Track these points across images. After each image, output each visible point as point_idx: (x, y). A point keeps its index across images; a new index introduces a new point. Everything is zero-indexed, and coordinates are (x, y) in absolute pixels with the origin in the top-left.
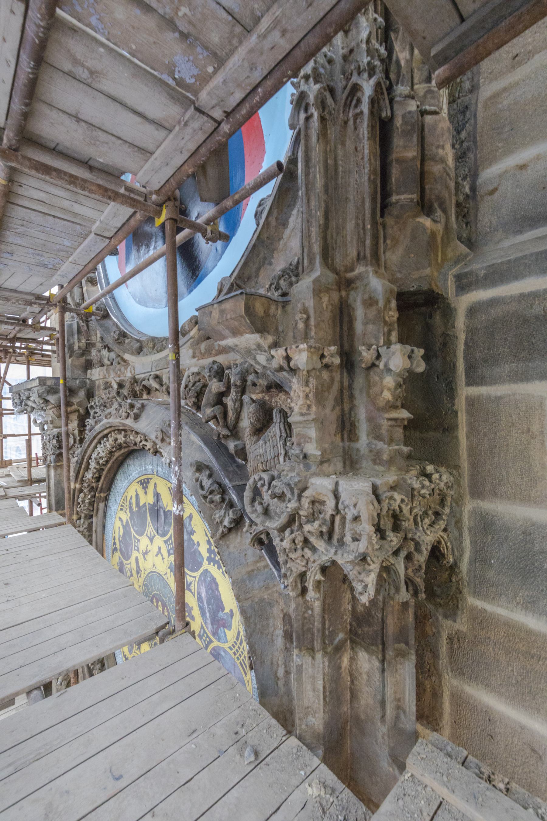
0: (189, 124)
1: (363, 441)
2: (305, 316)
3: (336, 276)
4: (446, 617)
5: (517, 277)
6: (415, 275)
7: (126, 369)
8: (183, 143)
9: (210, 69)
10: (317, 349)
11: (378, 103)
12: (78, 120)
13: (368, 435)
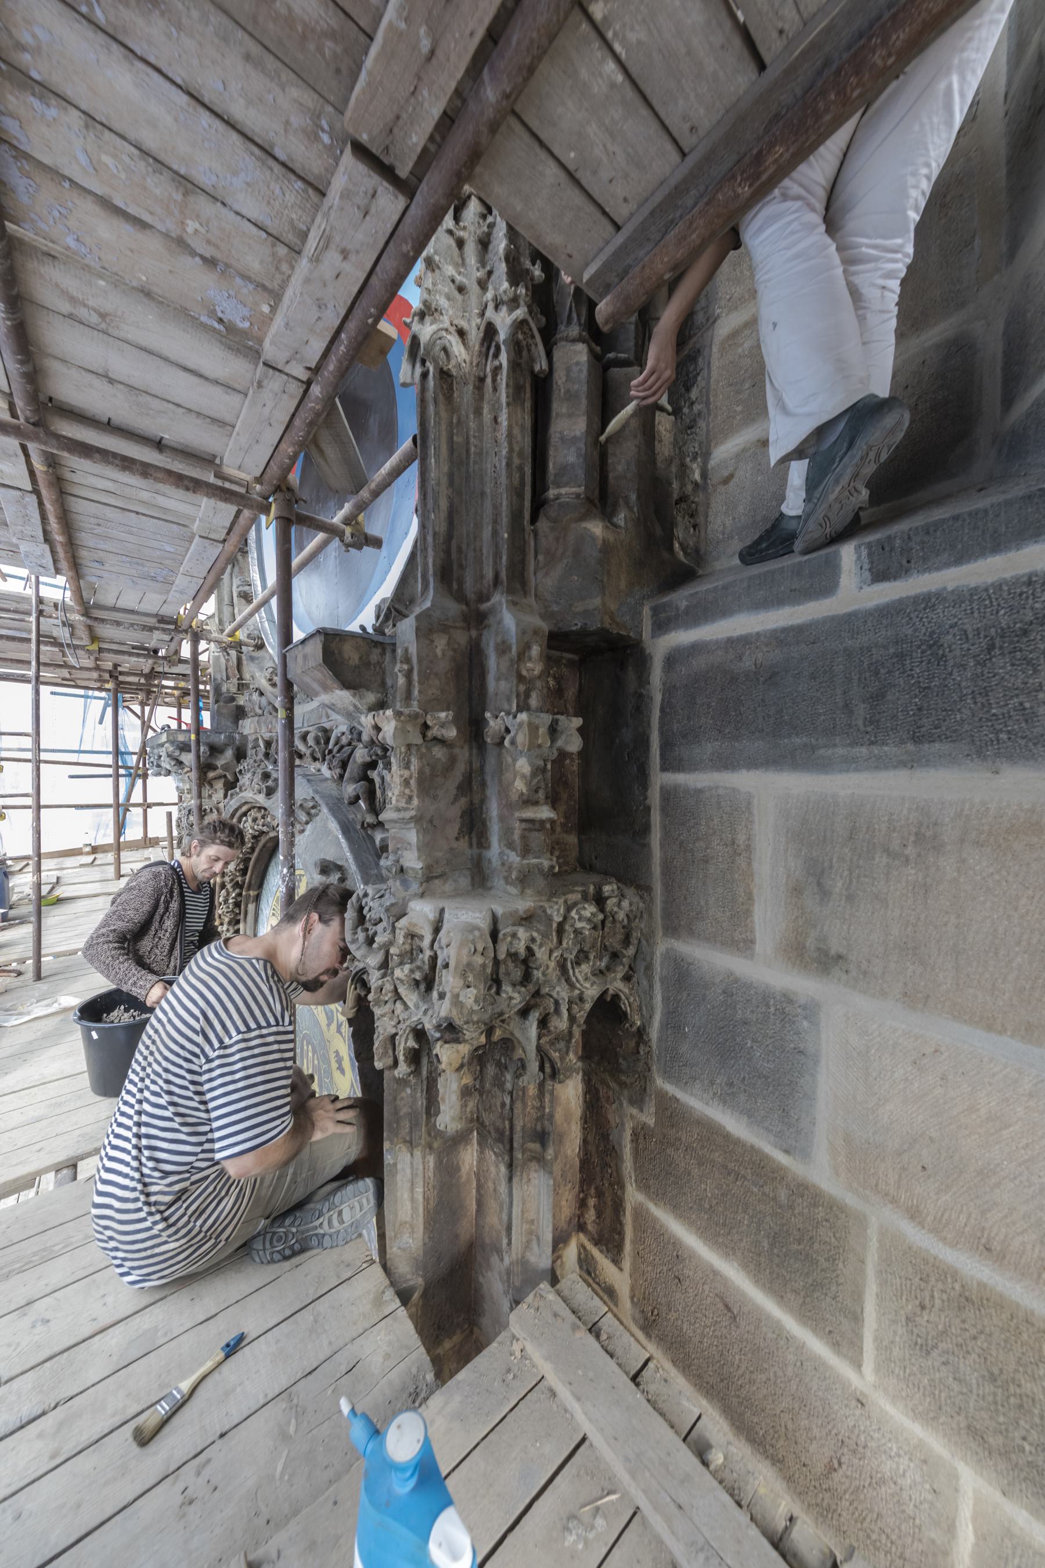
0: (265, 383)
1: (495, 849)
2: (406, 667)
3: (464, 607)
4: (632, 1102)
5: (725, 613)
6: (579, 607)
8: (266, 411)
9: (266, 309)
10: (416, 716)
11: (529, 351)
12: (111, 381)
13: (500, 841)
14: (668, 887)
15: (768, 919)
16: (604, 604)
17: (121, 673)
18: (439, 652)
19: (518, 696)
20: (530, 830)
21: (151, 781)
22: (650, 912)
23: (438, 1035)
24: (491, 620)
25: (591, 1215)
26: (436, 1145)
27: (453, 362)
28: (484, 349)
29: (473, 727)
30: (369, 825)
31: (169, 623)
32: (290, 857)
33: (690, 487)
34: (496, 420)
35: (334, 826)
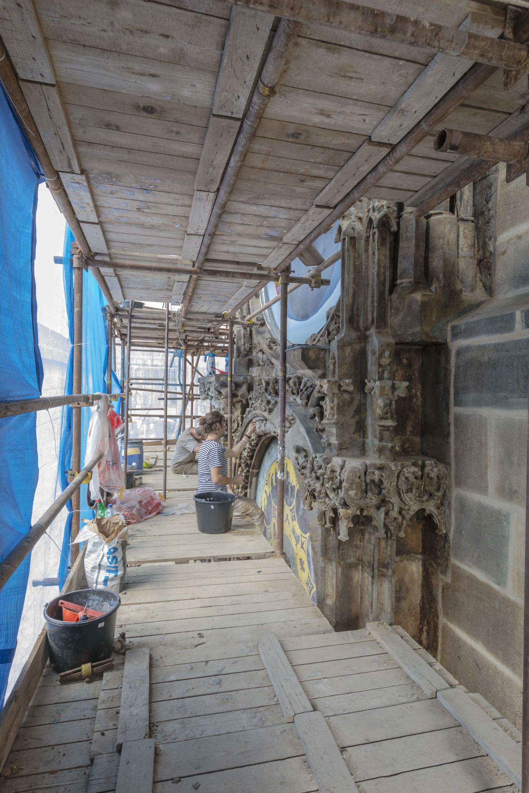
2: (333, 361)
5: (478, 334)
6: (410, 332)
7: (272, 370)
8: (281, 253)
10: (336, 382)
14: (457, 463)
15: (492, 477)
16: (422, 330)
17: (189, 340)
18: (347, 354)
19: (379, 373)
20: (383, 430)
21: (195, 402)
22: (449, 474)
23: (340, 507)
24: (370, 340)
25: (424, 635)
26: (342, 563)
27: (356, 232)
29: (361, 384)
30: (320, 430)
31: (220, 317)
32: (283, 442)
34: (374, 254)
35: (302, 430)
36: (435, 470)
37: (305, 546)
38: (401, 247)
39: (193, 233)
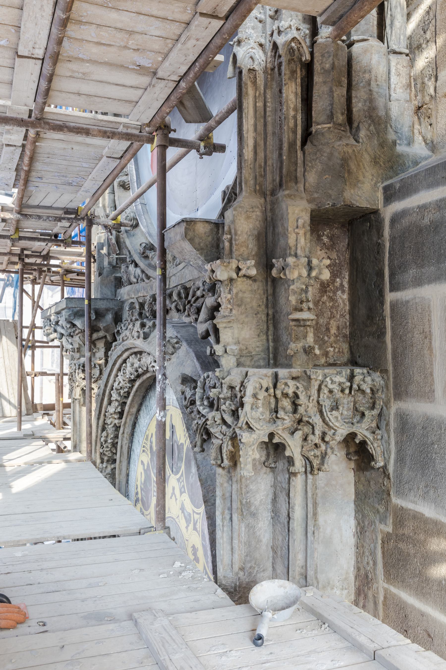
0: (156, 85)
5: (416, 191)
8: (156, 95)
11: (299, 50)
12: (79, 94)
17: (27, 256)
21: (38, 351)
27: (256, 63)
28: (273, 54)
31: (71, 213)
33: (427, 98)
36: (368, 379)
37: (198, 526)
38: (316, 83)
39: (26, 55)
